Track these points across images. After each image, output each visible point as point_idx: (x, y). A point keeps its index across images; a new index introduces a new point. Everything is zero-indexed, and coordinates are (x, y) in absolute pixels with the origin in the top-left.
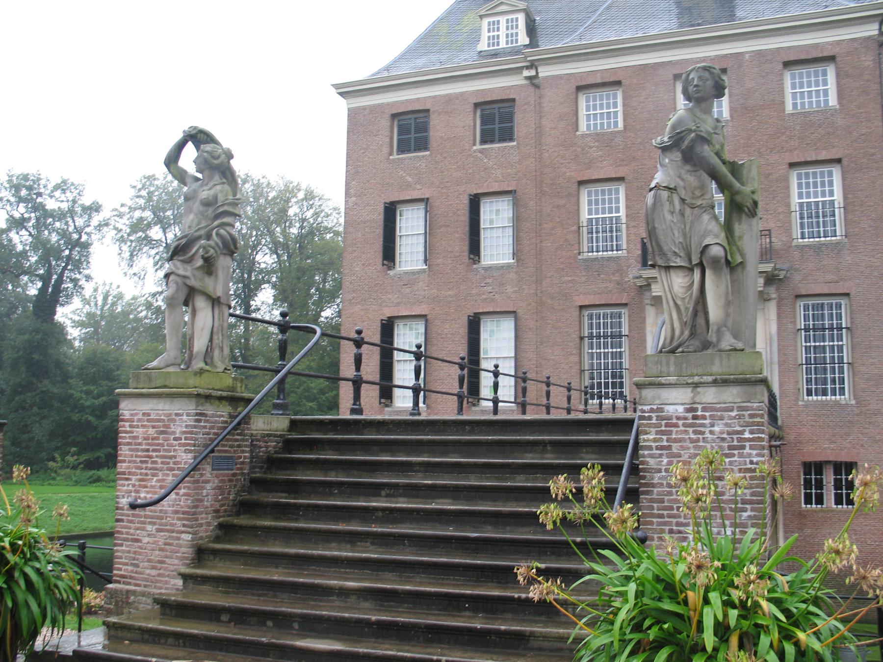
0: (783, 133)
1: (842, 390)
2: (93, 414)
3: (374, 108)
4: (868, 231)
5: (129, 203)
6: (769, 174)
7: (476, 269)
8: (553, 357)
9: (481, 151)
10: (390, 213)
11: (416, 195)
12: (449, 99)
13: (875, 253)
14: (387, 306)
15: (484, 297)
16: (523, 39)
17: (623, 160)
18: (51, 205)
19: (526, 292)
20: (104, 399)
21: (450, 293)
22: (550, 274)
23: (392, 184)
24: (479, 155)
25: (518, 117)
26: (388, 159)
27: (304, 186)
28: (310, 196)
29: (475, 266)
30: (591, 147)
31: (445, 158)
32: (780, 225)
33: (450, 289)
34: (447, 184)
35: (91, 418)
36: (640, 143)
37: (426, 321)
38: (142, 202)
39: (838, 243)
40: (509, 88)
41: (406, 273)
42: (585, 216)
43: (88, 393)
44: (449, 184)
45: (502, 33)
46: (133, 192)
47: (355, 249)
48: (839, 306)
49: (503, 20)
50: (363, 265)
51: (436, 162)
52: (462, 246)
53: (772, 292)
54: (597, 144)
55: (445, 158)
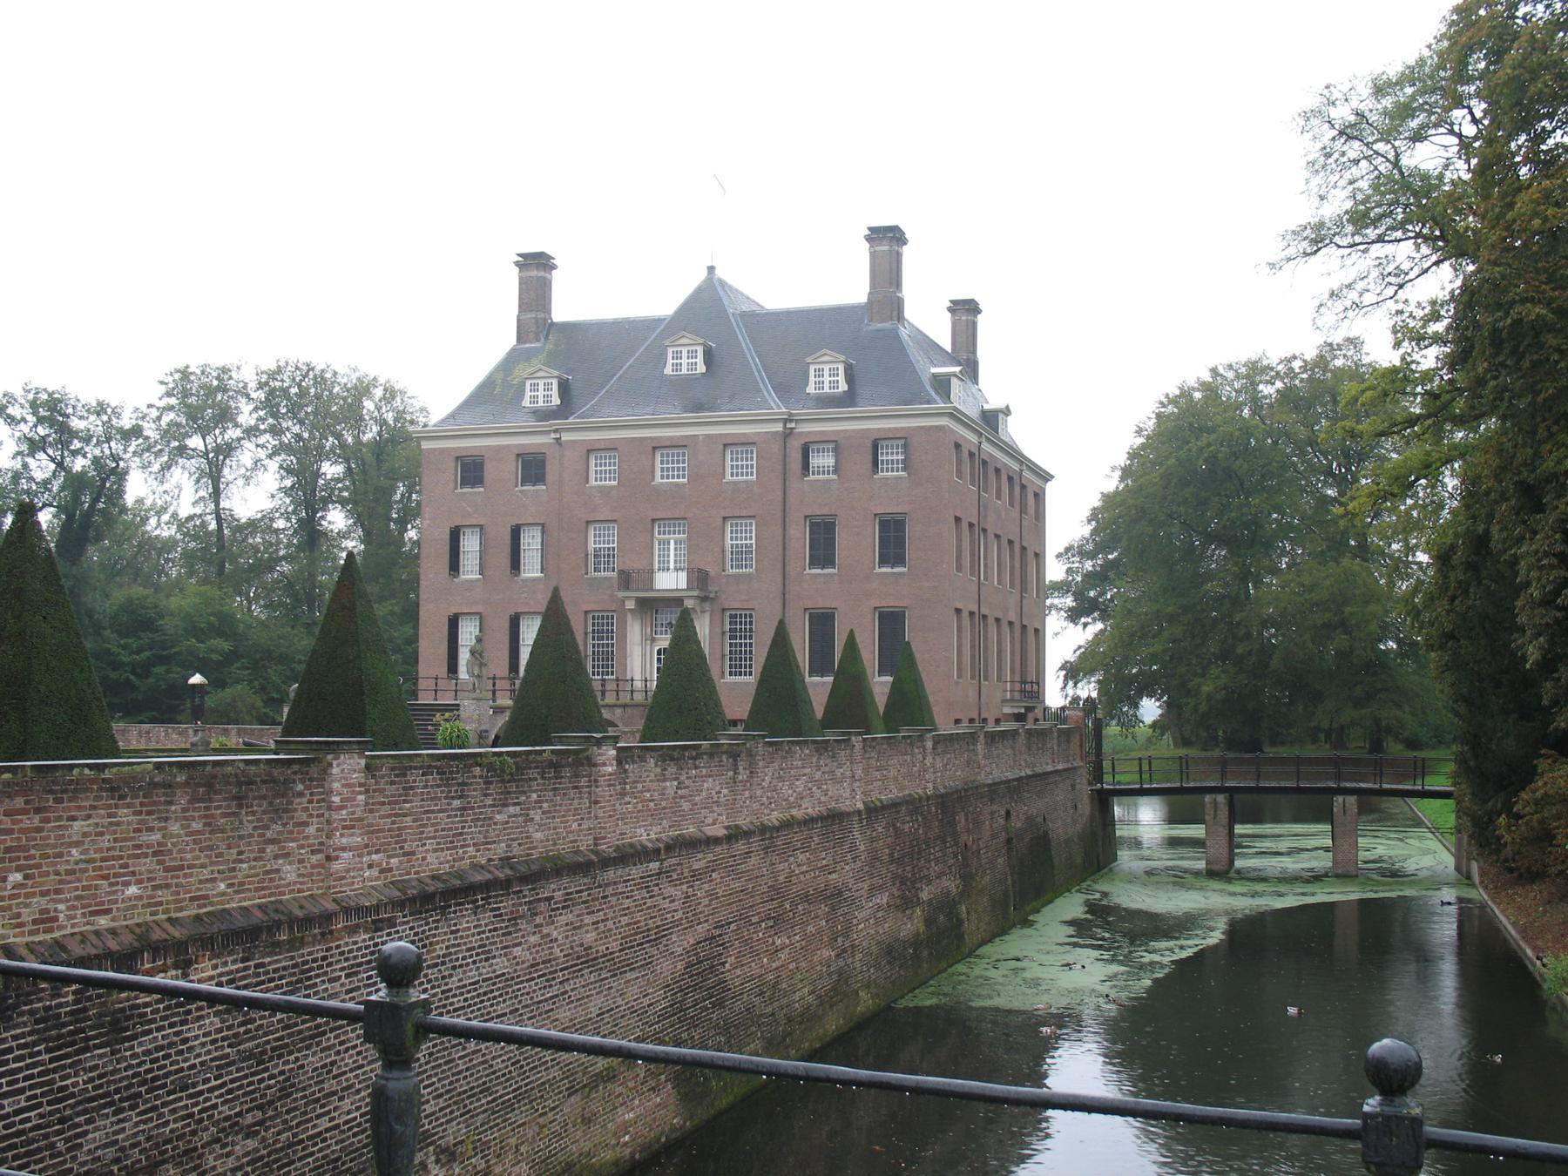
1: (751, 674)
2: (133, 672)
3: (442, 451)
5: (162, 404)
9: (522, 492)
10: (455, 536)
11: (475, 522)
12: (499, 449)
16: (556, 401)
18: (76, 424)
20: (148, 653)
25: (548, 467)
27: (382, 380)
28: (390, 394)
35: (132, 677)
37: (481, 618)
38: (173, 401)
39: (750, 575)
40: (542, 444)
41: (467, 581)
42: (591, 546)
43: (124, 647)
45: (541, 393)
46: (163, 389)
48: (751, 616)
49: (541, 382)
52: (506, 562)
53: (707, 606)
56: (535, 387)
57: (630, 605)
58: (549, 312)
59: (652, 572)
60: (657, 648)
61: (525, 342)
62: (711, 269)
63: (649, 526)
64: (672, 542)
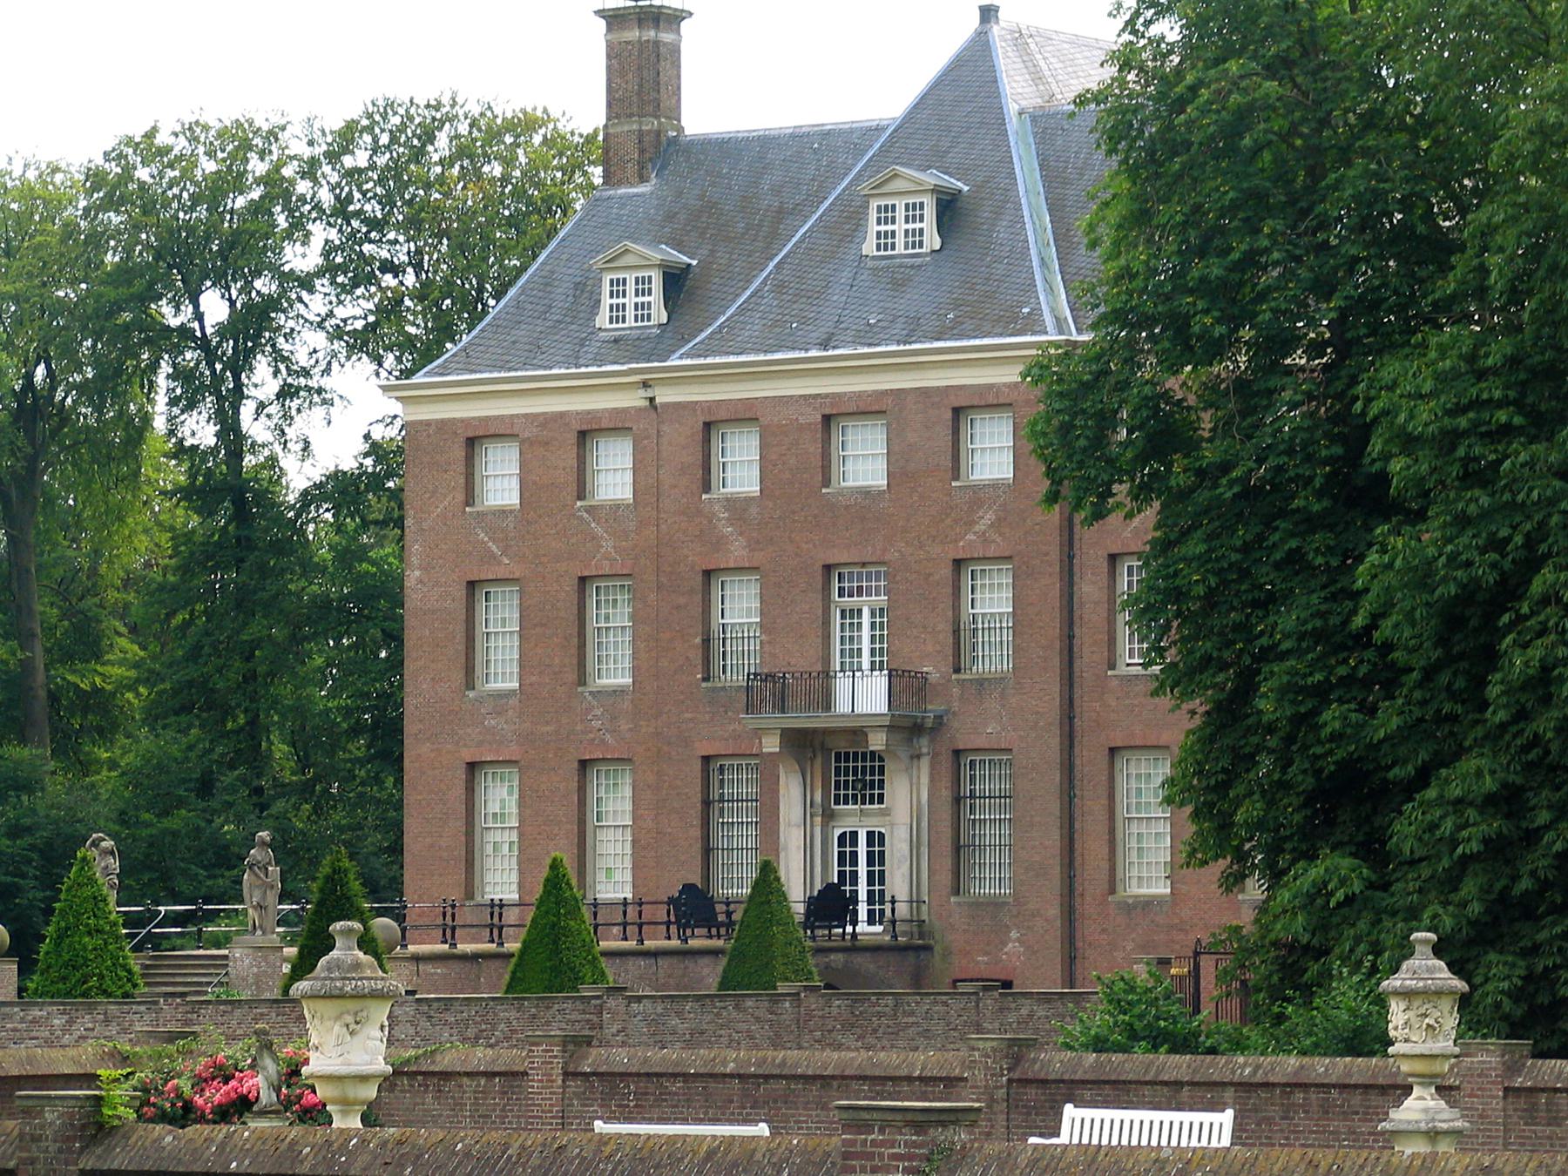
0: (948, 515)
3: (442, 425)
4: (1037, 663)
6: (930, 575)
7: (582, 693)
8: (669, 830)
13: (1041, 694)
14: (465, 745)
15: (591, 736)
17: (758, 542)
19: (644, 730)
21: (549, 728)
22: (666, 709)
23: (471, 553)
24: (585, 515)
26: (464, 512)
29: (580, 689)
30: (719, 520)
31: (540, 516)
32: (939, 648)
33: (547, 723)
34: (543, 559)
36: (780, 517)
44: (545, 559)
47: (421, 653)
49: (631, 277)
50: (433, 679)
51: (528, 522)
53: (924, 744)
54: (726, 515)
55: (540, 516)
56: (618, 287)
57: (771, 745)
58: (675, 113)
59: (827, 675)
60: (837, 832)
61: (619, 183)
62: (988, 14)
63: (819, 579)
64: (866, 612)
